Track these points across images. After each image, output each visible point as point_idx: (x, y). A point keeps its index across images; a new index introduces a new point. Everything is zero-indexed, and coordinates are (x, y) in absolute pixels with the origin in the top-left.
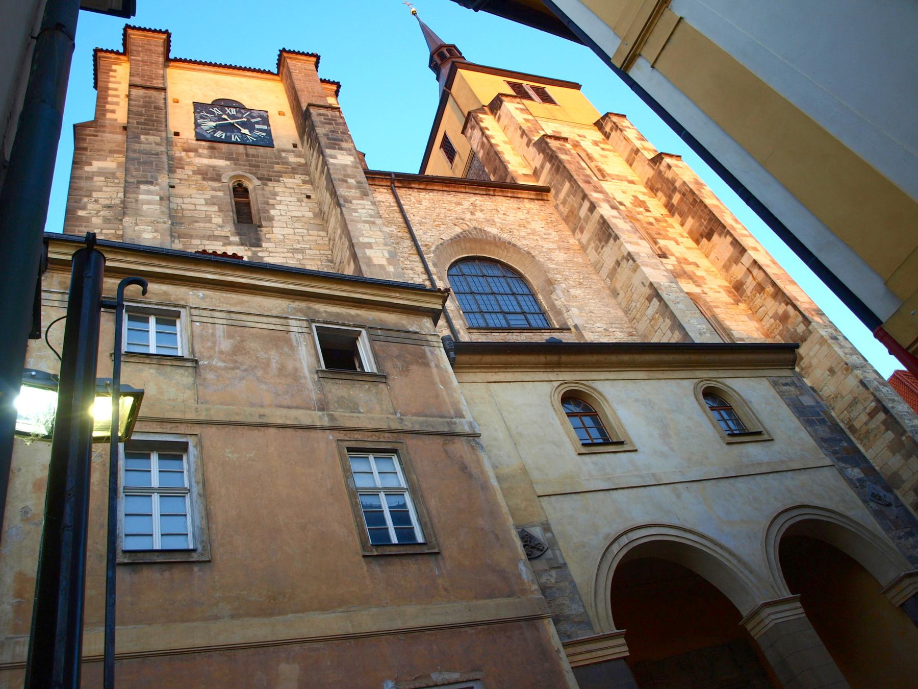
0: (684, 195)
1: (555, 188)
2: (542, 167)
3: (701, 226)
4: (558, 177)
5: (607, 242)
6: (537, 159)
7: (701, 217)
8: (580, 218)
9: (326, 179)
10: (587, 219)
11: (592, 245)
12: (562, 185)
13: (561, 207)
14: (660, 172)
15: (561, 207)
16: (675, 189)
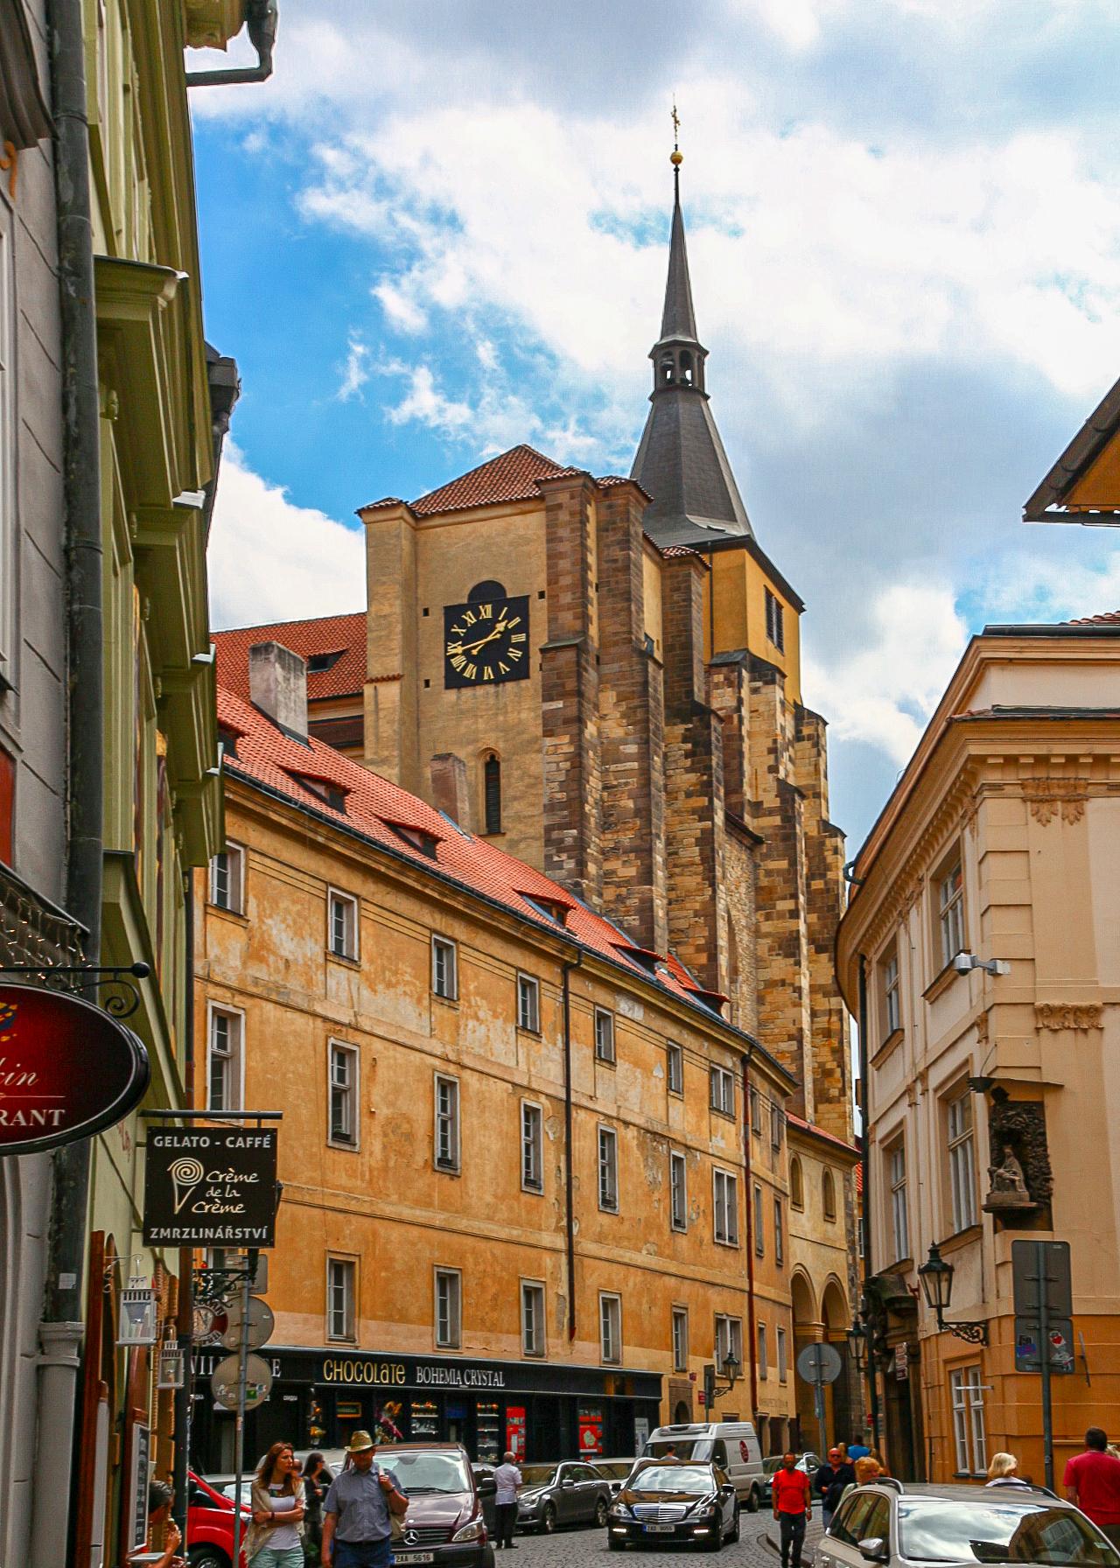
0: (828, 890)
1: (770, 847)
2: (771, 812)
3: (820, 933)
4: (781, 845)
5: (787, 956)
6: (771, 800)
7: (825, 926)
8: (774, 907)
9: (703, 831)
10: (781, 916)
11: (769, 941)
12: (781, 857)
13: (762, 872)
14: (823, 844)
15: (762, 872)
16: (823, 876)
